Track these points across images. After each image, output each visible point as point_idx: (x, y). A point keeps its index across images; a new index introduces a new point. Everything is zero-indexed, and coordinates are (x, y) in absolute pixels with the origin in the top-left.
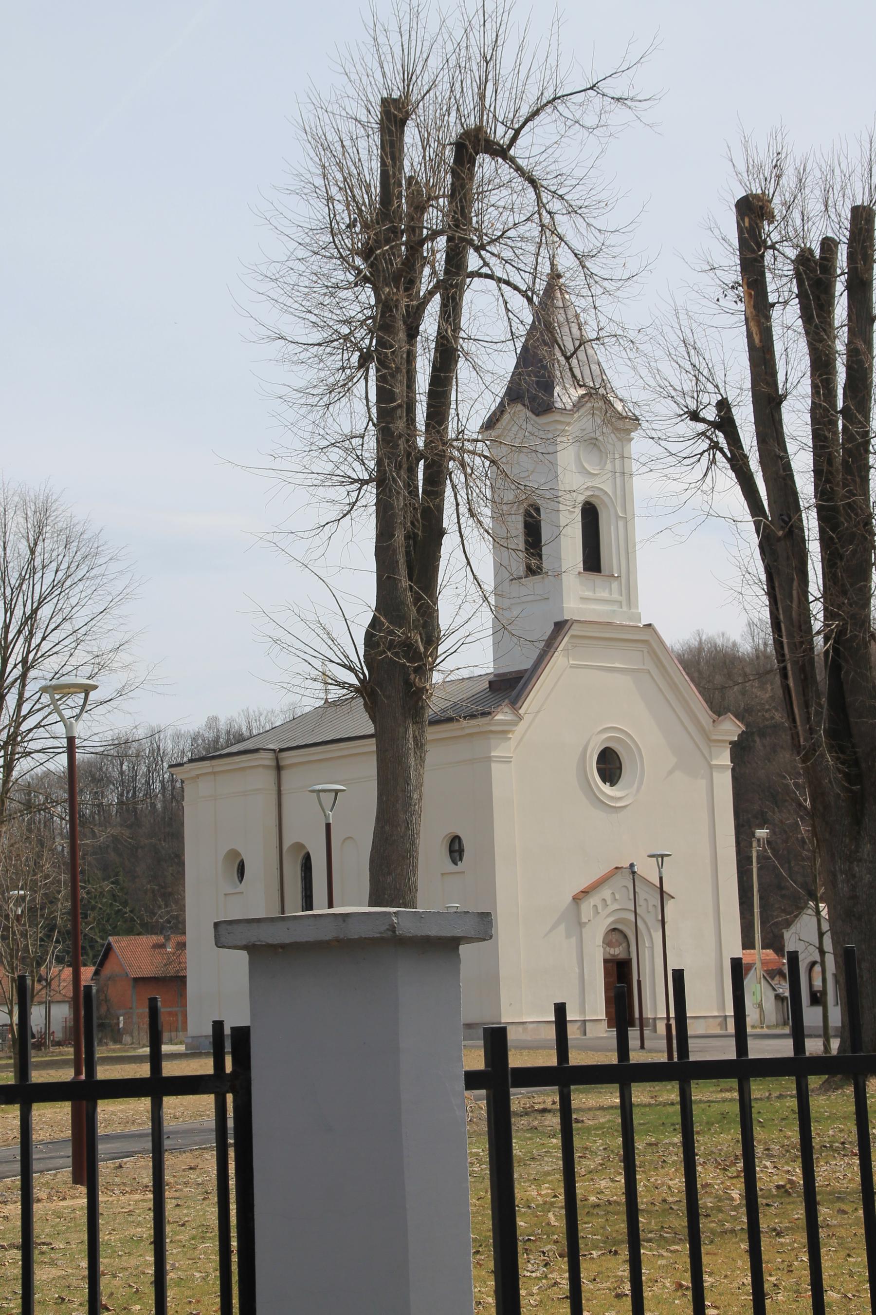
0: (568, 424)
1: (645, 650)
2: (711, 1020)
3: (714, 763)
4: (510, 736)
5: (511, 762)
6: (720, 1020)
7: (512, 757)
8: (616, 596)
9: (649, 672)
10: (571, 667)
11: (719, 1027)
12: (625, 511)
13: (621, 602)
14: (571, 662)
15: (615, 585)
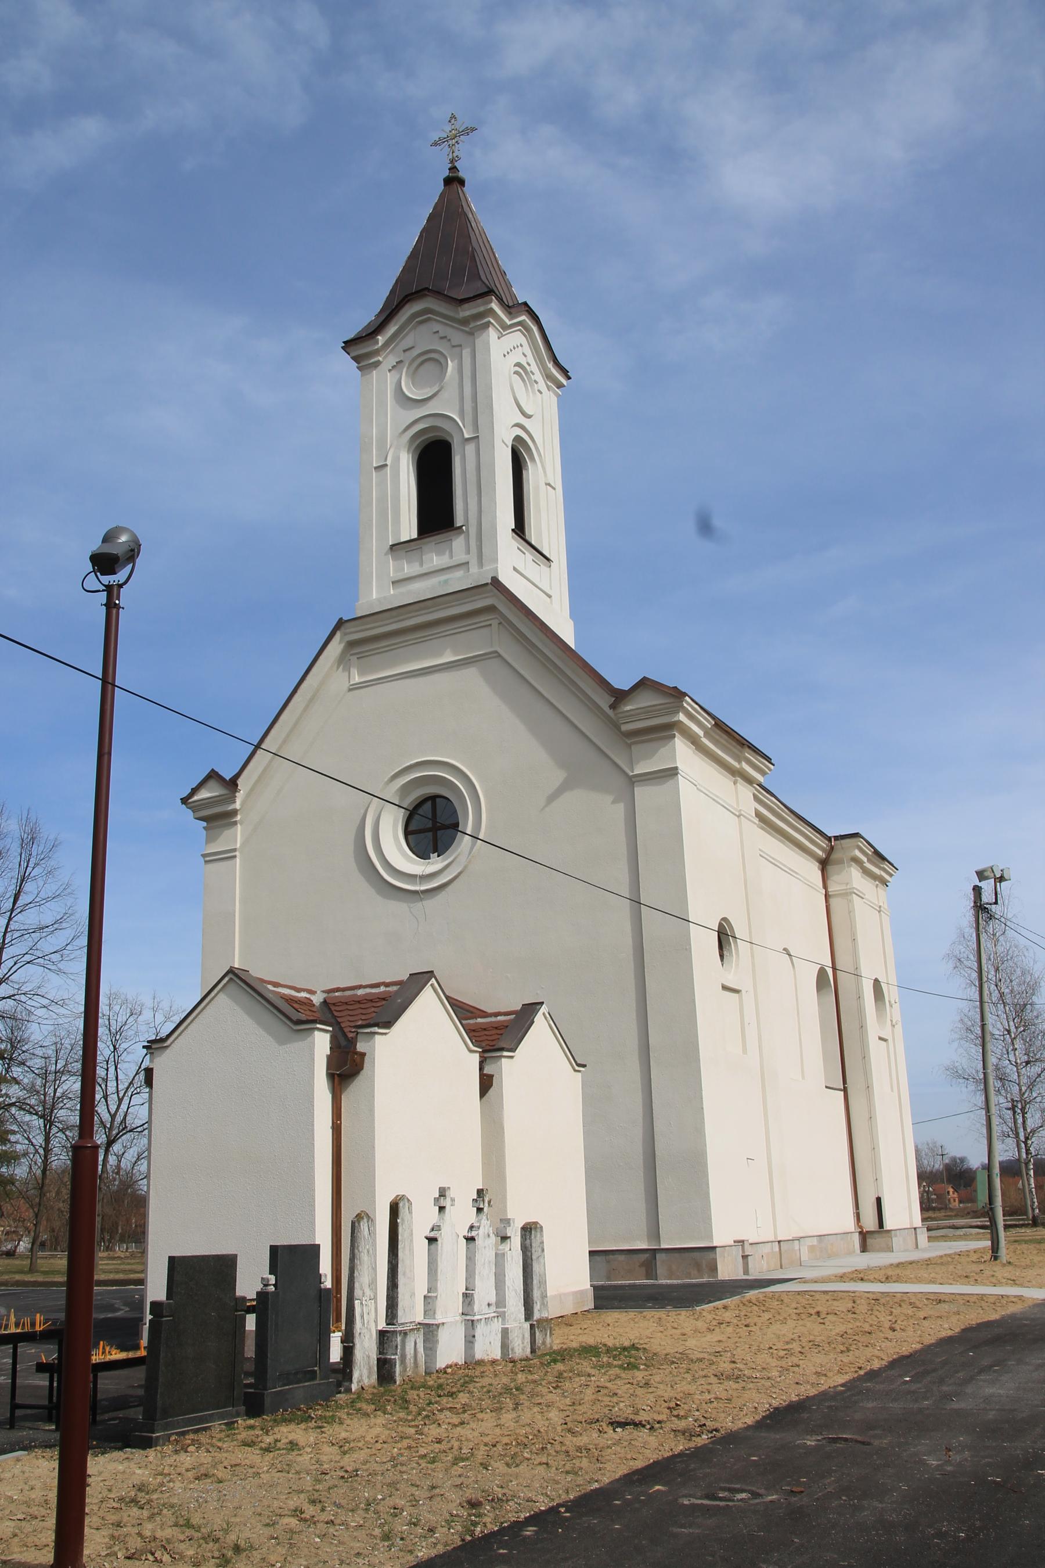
0: (377, 352)
1: (495, 623)
2: (621, 1258)
3: (639, 770)
4: (239, 817)
5: (235, 857)
6: (646, 1256)
7: (235, 850)
8: (460, 556)
9: (500, 656)
10: (350, 690)
11: (643, 1270)
12: (476, 426)
13: (468, 563)
14: (357, 679)
15: (458, 543)
